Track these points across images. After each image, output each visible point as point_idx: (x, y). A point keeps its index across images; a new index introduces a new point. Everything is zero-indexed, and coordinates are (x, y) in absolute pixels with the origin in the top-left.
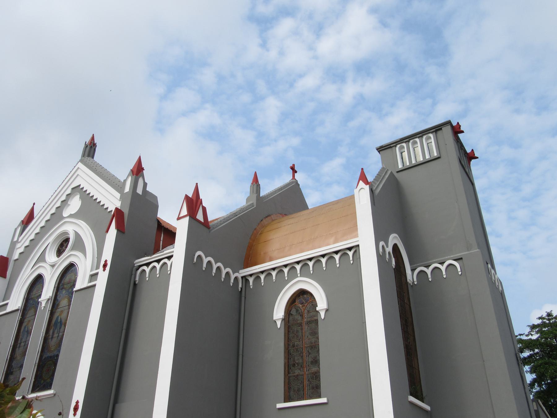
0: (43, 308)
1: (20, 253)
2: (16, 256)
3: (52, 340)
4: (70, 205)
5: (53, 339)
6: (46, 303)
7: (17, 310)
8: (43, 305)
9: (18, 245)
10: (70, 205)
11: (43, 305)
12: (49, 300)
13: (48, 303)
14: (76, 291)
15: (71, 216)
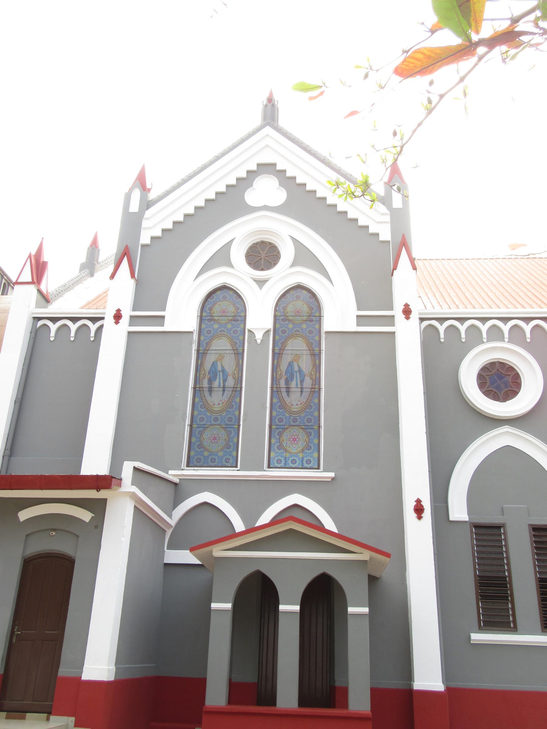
0: (259, 341)
1: (153, 238)
2: (145, 239)
3: (288, 395)
4: (255, 189)
5: (292, 395)
6: (264, 334)
7: (192, 332)
8: (259, 336)
9: (145, 224)
10: (255, 189)
11: (259, 336)
12: (268, 331)
13: (269, 336)
14: (327, 333)
15: (265, 208)
